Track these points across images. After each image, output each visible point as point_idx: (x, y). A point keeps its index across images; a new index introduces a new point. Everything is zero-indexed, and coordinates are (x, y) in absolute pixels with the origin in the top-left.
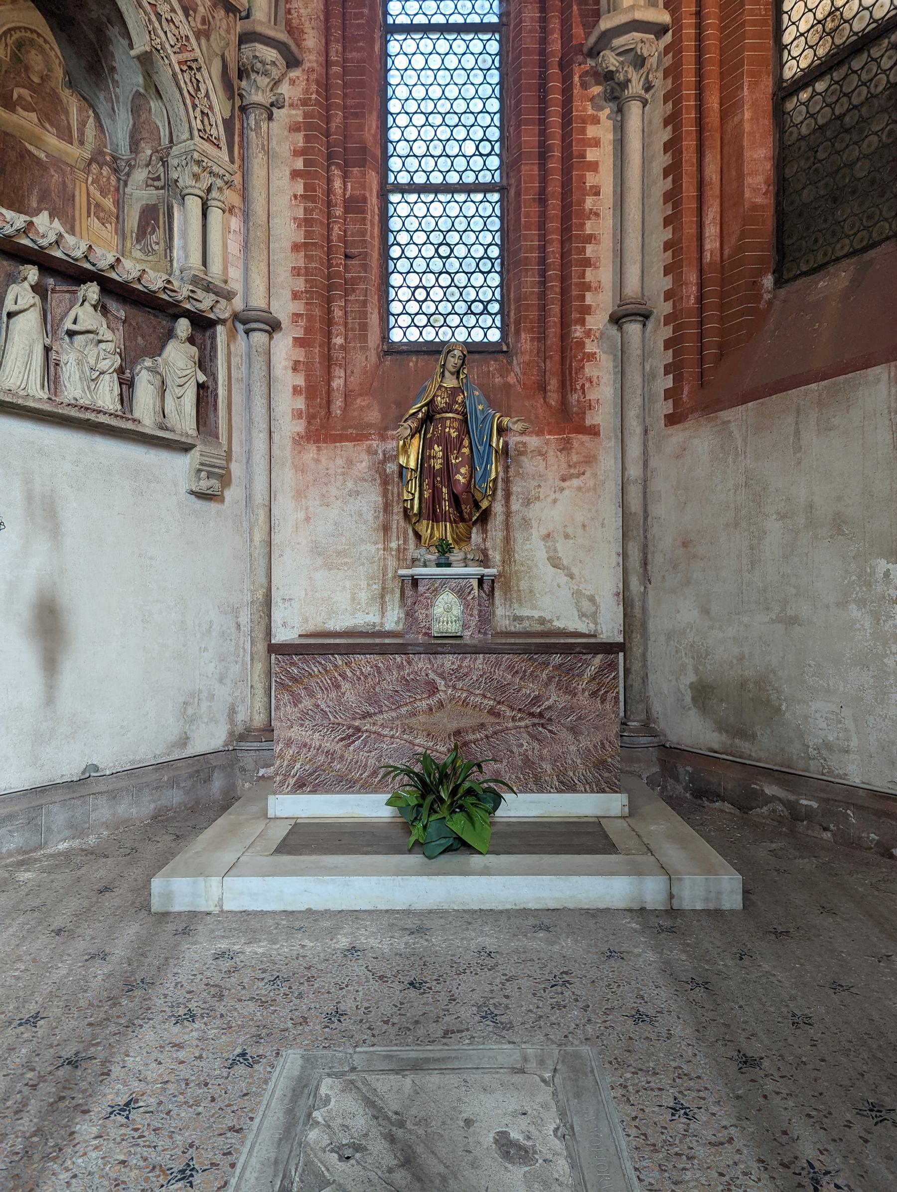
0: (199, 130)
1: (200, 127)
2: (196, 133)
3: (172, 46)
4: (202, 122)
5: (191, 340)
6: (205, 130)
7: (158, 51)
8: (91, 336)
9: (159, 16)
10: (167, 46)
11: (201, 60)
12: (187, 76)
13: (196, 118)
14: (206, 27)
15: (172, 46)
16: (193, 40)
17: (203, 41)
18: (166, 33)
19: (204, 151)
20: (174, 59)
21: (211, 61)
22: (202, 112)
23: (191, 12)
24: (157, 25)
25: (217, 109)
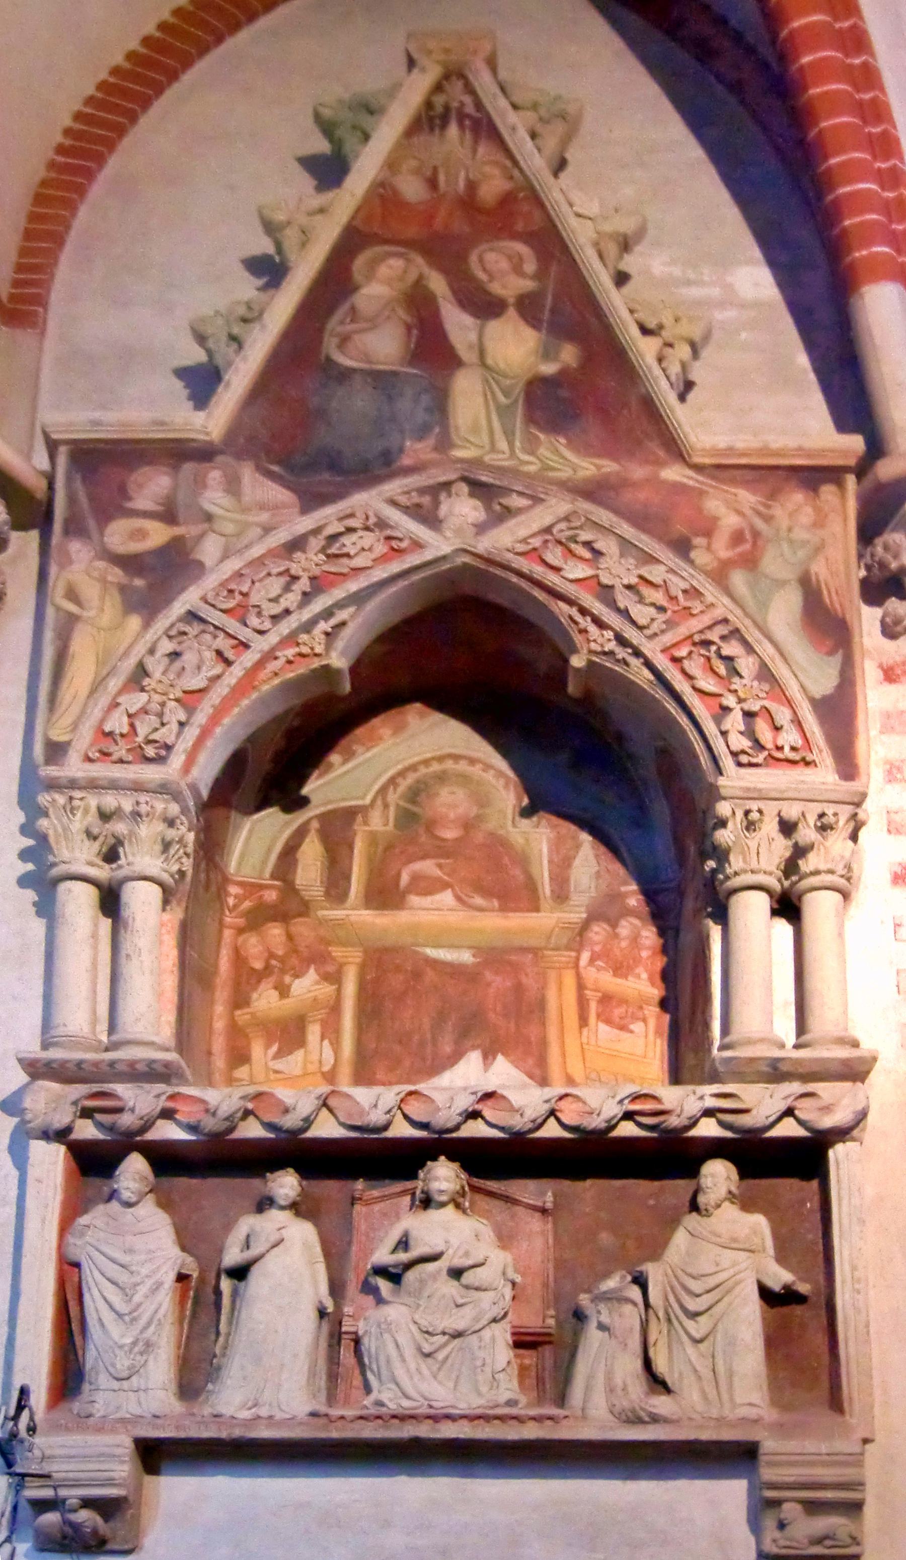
0: (734, 754)
1: (740, 742)
2: (727, 762)
3: (641, 628)
4: (750, 733)
5: (747, 1204)
6: (759, 745)
7: (611, 653)
8: (431, 1267)
9: (605, 592)
10: (631, 634)
11: (738, 619)
12: (694, 666)
13: (724, 734)
14: (747, 546)
15: (641, 628)
16: (711, 592)
17: (738, 579)
18: (625, 613)
19: (748, 789)
20: (651, 649)
21: (764, 606)
22: (749, 715)
23: (698, 541)
24: (598, 608)
25: (793, 690)
